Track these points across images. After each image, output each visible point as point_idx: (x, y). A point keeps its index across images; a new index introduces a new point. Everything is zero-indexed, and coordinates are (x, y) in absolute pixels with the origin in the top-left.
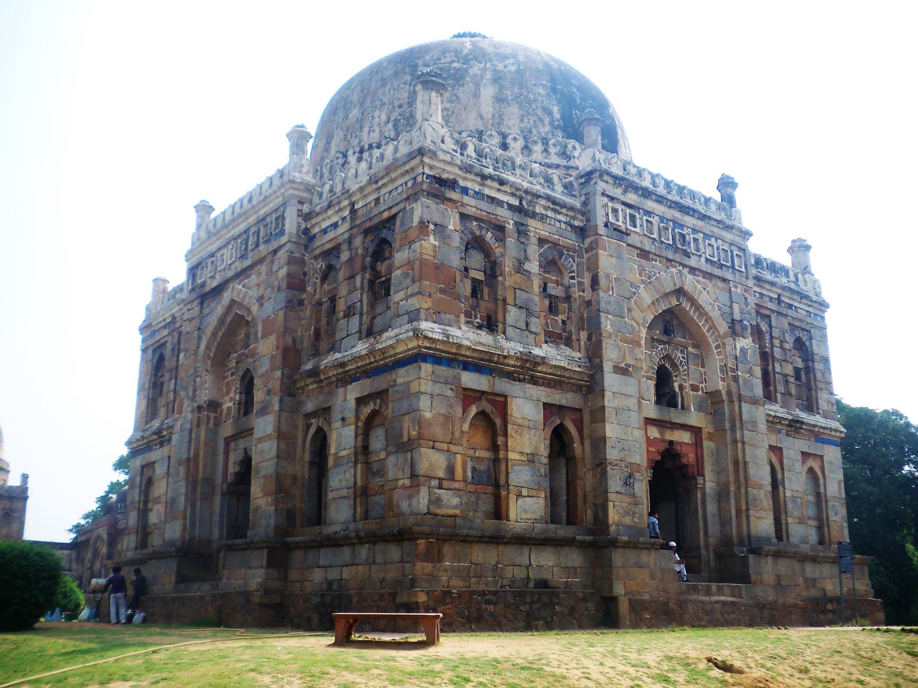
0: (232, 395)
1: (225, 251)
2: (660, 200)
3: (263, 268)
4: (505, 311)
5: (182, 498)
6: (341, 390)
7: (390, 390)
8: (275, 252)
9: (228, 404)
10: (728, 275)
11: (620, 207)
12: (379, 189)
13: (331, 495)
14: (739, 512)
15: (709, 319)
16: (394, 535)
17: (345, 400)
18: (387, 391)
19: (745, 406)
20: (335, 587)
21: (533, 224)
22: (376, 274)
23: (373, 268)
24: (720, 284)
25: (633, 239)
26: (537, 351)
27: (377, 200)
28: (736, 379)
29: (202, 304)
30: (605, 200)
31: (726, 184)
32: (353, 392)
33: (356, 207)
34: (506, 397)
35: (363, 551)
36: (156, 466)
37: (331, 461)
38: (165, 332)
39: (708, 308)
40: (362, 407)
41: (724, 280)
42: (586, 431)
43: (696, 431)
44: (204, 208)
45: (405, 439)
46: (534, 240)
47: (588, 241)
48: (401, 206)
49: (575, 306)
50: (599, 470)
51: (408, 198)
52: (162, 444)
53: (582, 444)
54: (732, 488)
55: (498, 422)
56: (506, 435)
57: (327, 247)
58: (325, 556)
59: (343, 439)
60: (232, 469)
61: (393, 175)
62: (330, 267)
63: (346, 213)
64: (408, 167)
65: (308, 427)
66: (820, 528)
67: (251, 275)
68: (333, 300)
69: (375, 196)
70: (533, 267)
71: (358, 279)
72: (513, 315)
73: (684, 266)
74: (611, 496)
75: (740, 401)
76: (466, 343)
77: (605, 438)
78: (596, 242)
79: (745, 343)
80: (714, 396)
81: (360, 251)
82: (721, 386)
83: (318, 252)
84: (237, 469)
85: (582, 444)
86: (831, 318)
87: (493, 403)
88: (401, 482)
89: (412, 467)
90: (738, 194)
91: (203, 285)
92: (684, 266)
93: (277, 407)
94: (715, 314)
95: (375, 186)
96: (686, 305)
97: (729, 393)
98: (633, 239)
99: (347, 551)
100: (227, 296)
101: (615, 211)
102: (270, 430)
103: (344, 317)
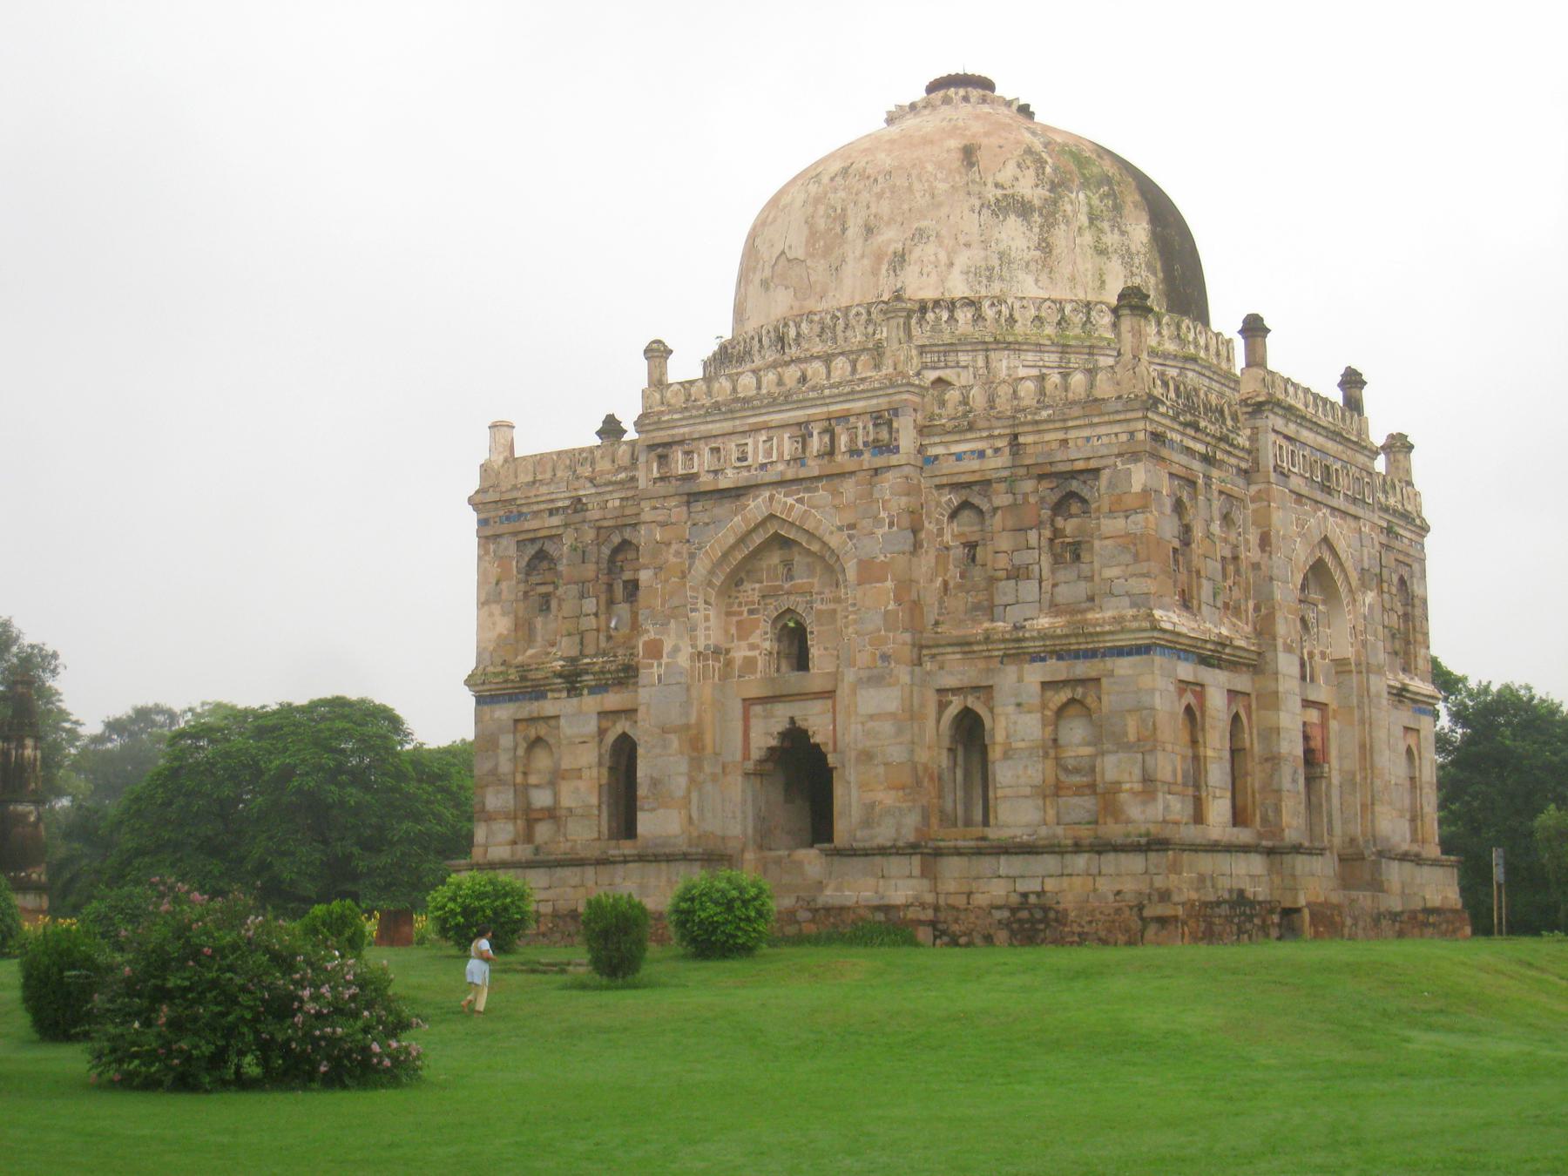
0: (755, 638)
1: (750, 441)
2: (1314, 426)
3: (849, 488)
4: (1199, 587)
5: (682, 781)
6: (1011, 671)
7: (1104, 681)
8: (876, 471)
9: (740, 653)
10: (1359, 512)
11: (1284, 443)
12: (1067, 429)
13: (1000, 793)
14: (1363, 806)
15: (1343, 570)
16: (1139, 844)
17: (1020, 680)
18: (1098, 680)
19: (1373, 678)
20: (1032, 899)
21: (1215, 473)
22: (1057, 533)
23: (1052, 524)
24: (1353, 524)
25: (1296, 482)
26: (1225, 632)
27: (1065, 442)
28: (1364, 644)
29: (688, 503)
30: (1273, 437)
31: (1352, 381)
32: (1035, 674)
33: (1021, 440)
34: (1202, 686)
35: (1081, 862)
36: (562, 721)
37: (995, 753)
38: (555, 520)
39: (1343, 556)
40: (1049, 694)
41: (1356, 518)
42: (1254, 717)
43: (1321, 706)
44: (657, 353)
46: (1216, 494)
47: (1253, 489)
48: (1110, 461)
49: (1243, 569)
50: (1268, 765)
51: (1120, 455)
52: (573, 689)
53: (1251, 734)
54: (1358, 778)
55: (1198, 714)
56: (1203, 729)
57: (963, 479)
58: (1006, 865)
59: (1016, 724)
61: (1096, 420)
62: (965, 505)
64: (1122, 417)
65: (942, 706)
66: (1413, 820)
68: (972, 546)
69: (1061, 435)
70: (1216, 527)
71: (1033, 536)
72: (1206, 589)
73: (1327, 506)
74: (1285, 794)
75: (1368, 672)
76: (1184, 630)
77: (1278, 730)
78: (1268, 491)
79: (1370, 597)
80: (1341, 665)
82: (1349, 652)
83: (945, 480)
84: (773, 743)
85: (1251, 734)
86: (1432, 544)
87: (1194, 692)
88: (1127, 786)
89: (1144, 769)
90: (1368, 396)
91: (694, 476)
92: (1327, 506)
93: (905, 678)
94: (1349, 565)
95: (1058, 425)
96: (1327, 558)
97: (1358, 664)
98: (1296, 482)
99: (1050, 863)
100: (756, 506)
101: (1281, 447)
103: (1008, 578)
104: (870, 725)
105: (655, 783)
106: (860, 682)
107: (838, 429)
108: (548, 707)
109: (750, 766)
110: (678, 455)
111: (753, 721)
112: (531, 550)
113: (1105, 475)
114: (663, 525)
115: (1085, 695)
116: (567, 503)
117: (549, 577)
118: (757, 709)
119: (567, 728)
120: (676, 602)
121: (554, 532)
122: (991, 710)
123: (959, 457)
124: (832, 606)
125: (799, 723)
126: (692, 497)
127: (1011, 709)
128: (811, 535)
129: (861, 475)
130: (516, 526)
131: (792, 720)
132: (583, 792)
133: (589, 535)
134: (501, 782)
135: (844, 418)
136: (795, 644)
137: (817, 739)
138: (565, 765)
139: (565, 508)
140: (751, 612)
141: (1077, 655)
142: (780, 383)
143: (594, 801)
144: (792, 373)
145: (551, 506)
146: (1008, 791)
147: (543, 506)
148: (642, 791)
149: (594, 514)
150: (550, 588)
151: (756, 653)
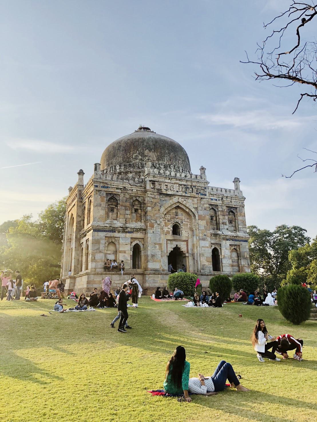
3: (195, 200)
5: (160, 256)
6: (224, 241)
17: (226, 244)
32: (228, 243)
33: (223, 199)
36: (120, 239)
38: (119, 191)
45: (246, 257)
60: (170, 249)
63: (220, 199)
65: (212, 246)
67: (188, 199)
71: (226, 216)
81: (226, 210)
100: (175, 199)
102: (208, 245)
104: (203, 249)
105: (153, 256)
106: (200, 239)
107: (194, 188)
108: (116, 234)
109: (168, 254)
110: (156, 183)
111: (168, 244)
112: (109, 197)
113: (238, 209)
114: (153, 198)
115: (237, 248)
116: (122, 187)
117: (114, 204)
118: (169, 242)
119: (121, 241)
120: (157, 216)
121: (118, 193)
122: (221, 249)
123: (212, 199)
124: (187, 223)
125: (178, 246)
126: (161, 194)
127: (224, 249)
128: (187, 207)
129: (198, 198)
130: (106, 189)
131: (177, 245)
132: (125, 256)
133: (128, 196)
134: (100, 252)
135: (195, 186)
136: (176, 230)
137: (182, 250)
138: (120, 250)
139: (121, 189)
140: (168, 221)
141: (236, 240)
142: (181, 176)
143: (129, 259)
144: (183, 175)
145: (117, 187)
146: (224, 265)
147: (114, 187)
148: (149, 258)
149: (131, 192)
150: (114, 206)
151: (170, 230)
